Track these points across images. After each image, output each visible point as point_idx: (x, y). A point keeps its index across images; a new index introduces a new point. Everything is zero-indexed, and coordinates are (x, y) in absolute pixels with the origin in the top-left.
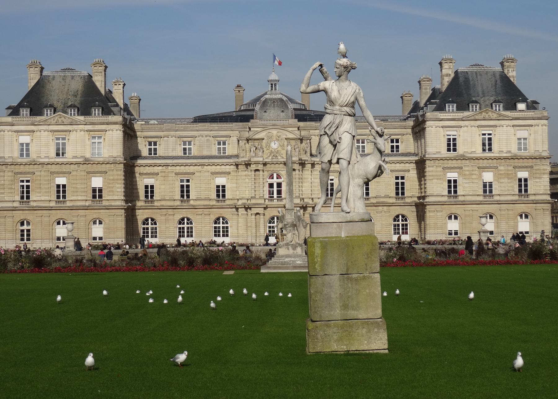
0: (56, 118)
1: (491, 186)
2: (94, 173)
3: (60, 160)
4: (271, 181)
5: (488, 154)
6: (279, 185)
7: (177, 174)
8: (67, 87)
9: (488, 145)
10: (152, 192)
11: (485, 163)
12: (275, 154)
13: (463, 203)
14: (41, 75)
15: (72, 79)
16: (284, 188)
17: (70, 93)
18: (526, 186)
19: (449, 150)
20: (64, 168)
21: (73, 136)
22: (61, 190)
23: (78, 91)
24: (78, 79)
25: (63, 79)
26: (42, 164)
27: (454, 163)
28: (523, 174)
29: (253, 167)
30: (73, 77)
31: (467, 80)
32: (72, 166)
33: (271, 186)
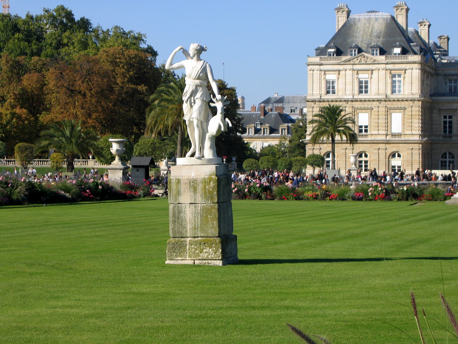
0: (360, 58)
2: (394, 109)
3: (363, 96)
8: (371, 28)
10: (450, 127)
14: (348, 17)
15: (376, 20)
17: (374, 34)
20: (367, 105)
23: (380, 32)
24: (381, 21)
25: (368, 21)
30: (376, 19)
32: (375, 103)
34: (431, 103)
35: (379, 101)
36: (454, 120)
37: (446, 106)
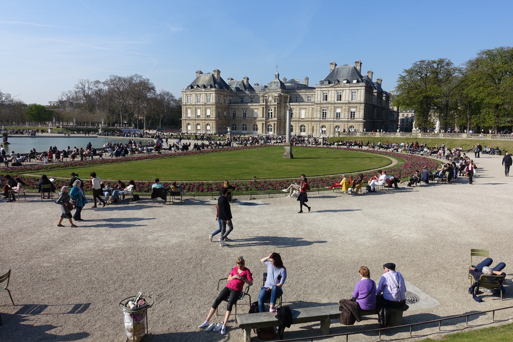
1: (340, 115)
6: (272, 113)
9: (340, 98)
11: (338, 105)
16: (273, 114)
18: (354, 115)
19: (324, 100)
20: (199, 106)
26: (193, 105)
27: (326, 105)
28: (353, 110)
31: (338, 71)
33: (269, 113)
35: (203, 105)
37: (234, 107)
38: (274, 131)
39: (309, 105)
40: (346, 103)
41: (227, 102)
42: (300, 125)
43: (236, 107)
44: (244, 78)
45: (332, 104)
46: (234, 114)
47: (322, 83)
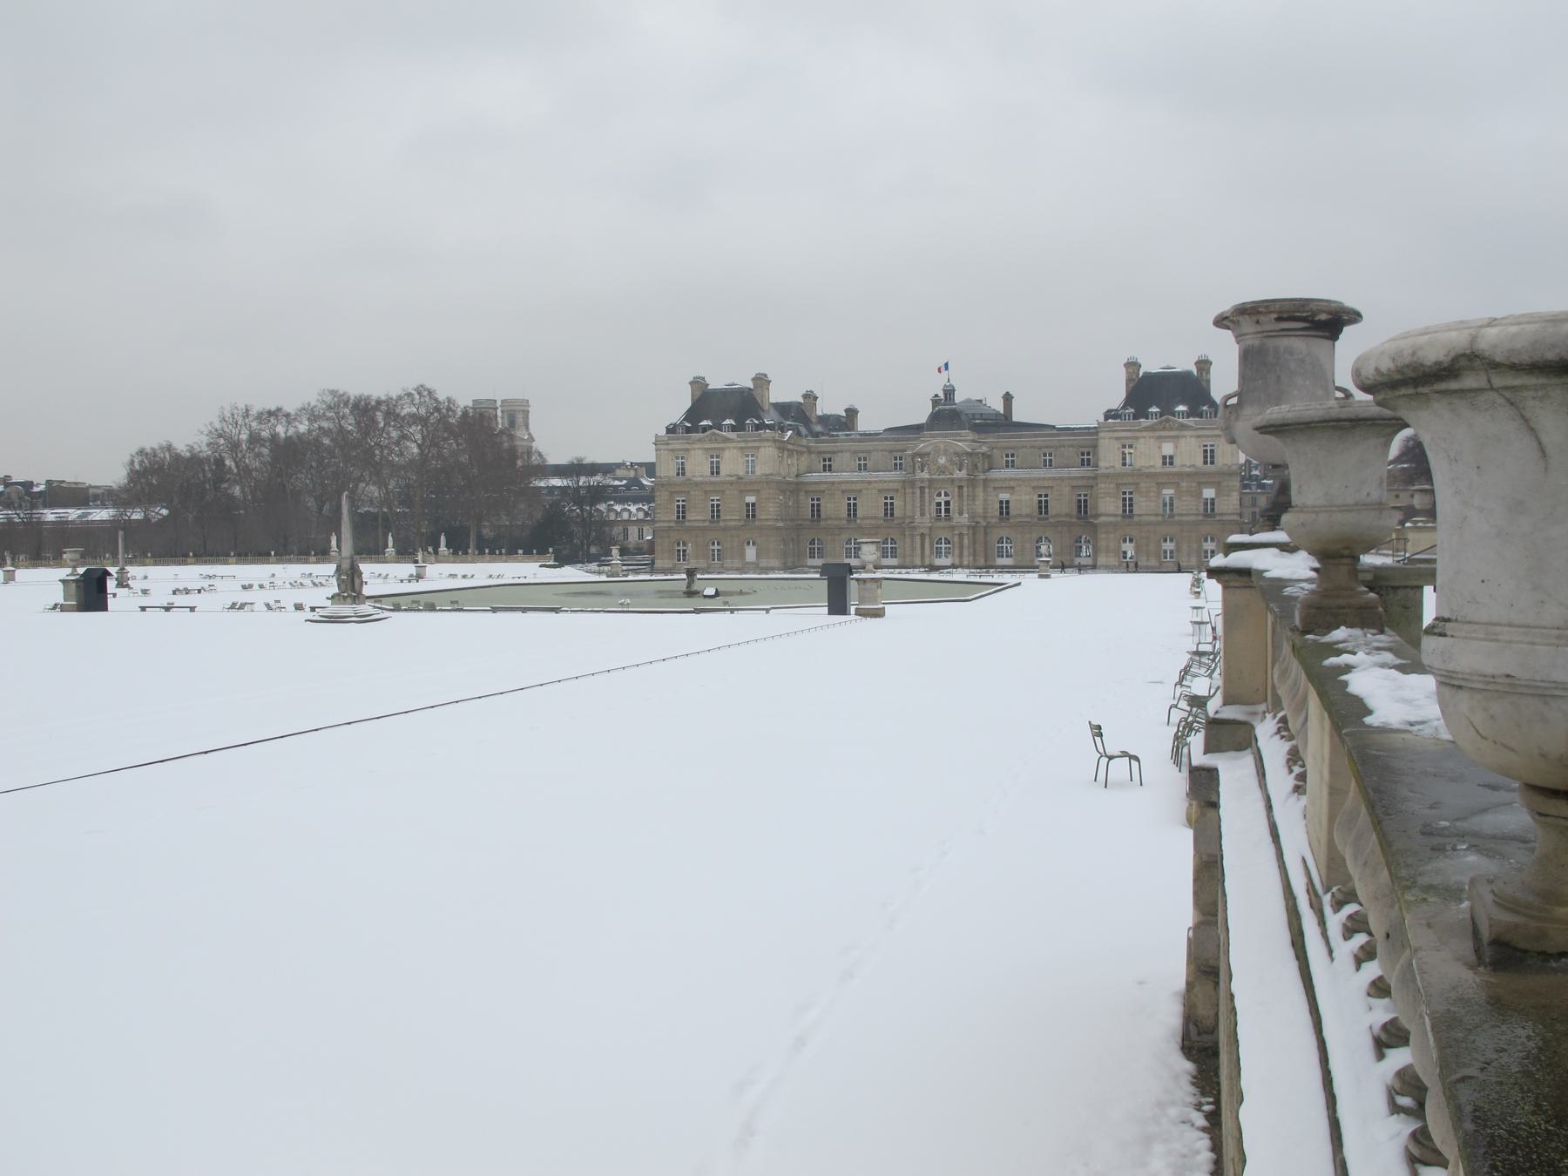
4: (938, 500)
5: (1168, 469)
6: (947, 503)
7: (843, 492)
12: (942, 470)
13: (1139, 524)
21: (727, 454)
22: (716, 512)
26: (697, 484)
29: (918, 484)
33: (939, 504)
34: (798, 484)
35: (731, 483)
36: (822, 502)
38: (961, 555)
39: (1062, 479)
40: (1189, 475)
41: (794, 470)
42: (1035, 536)
43: (822, 487)
44: (805, 396)
45: (1149, 475)
46: (816, 511)
47: (1109, 415)
